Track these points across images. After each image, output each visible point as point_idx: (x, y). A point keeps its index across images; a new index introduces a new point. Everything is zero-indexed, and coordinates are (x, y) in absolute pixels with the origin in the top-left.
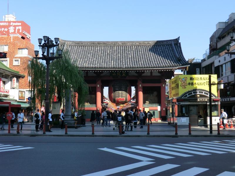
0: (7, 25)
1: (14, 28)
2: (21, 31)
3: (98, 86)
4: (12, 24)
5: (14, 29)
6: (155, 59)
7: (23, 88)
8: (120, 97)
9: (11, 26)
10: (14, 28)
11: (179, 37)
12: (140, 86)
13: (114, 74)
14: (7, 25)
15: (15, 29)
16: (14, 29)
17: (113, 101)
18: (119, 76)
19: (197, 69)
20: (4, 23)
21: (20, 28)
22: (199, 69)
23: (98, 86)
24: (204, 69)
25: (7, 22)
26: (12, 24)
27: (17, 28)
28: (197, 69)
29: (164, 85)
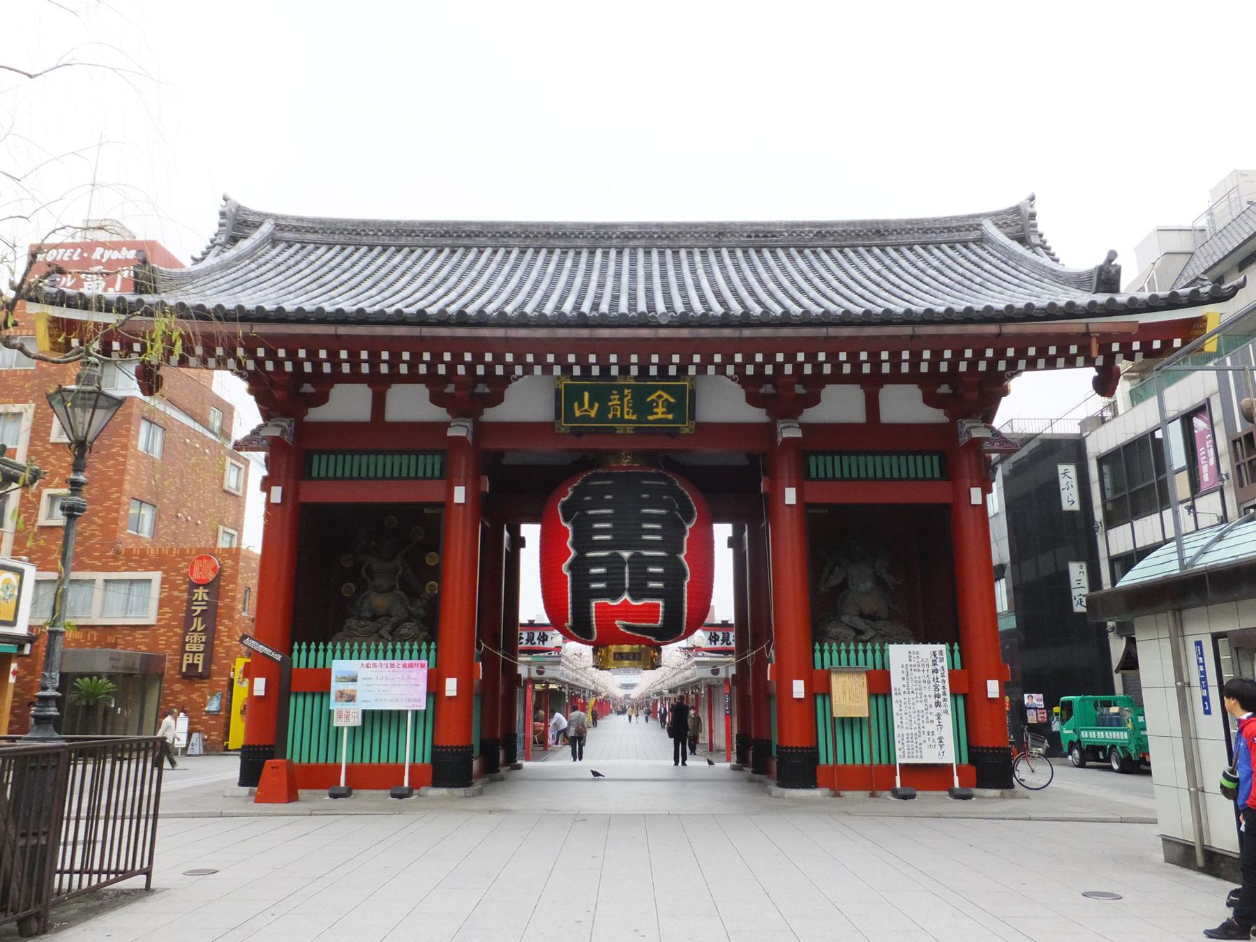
0: (76, 258)
3: (459, 495)
4: (102, 256)
6: (914, 271)
7: (94, 568)
11: (1032, 199)
12: (790, 496)
13: (581, 405)
14: (76, 258)
17: (569, 624)
18: (622, 420)
19: (1061, 468)
20: (62, 251)
22: (1072, 469)
23: (459, 495)
24: (1106, 469)
25: (74, 246)
26: (102, 256)
28: (1061, 468)
29: (976, 495)
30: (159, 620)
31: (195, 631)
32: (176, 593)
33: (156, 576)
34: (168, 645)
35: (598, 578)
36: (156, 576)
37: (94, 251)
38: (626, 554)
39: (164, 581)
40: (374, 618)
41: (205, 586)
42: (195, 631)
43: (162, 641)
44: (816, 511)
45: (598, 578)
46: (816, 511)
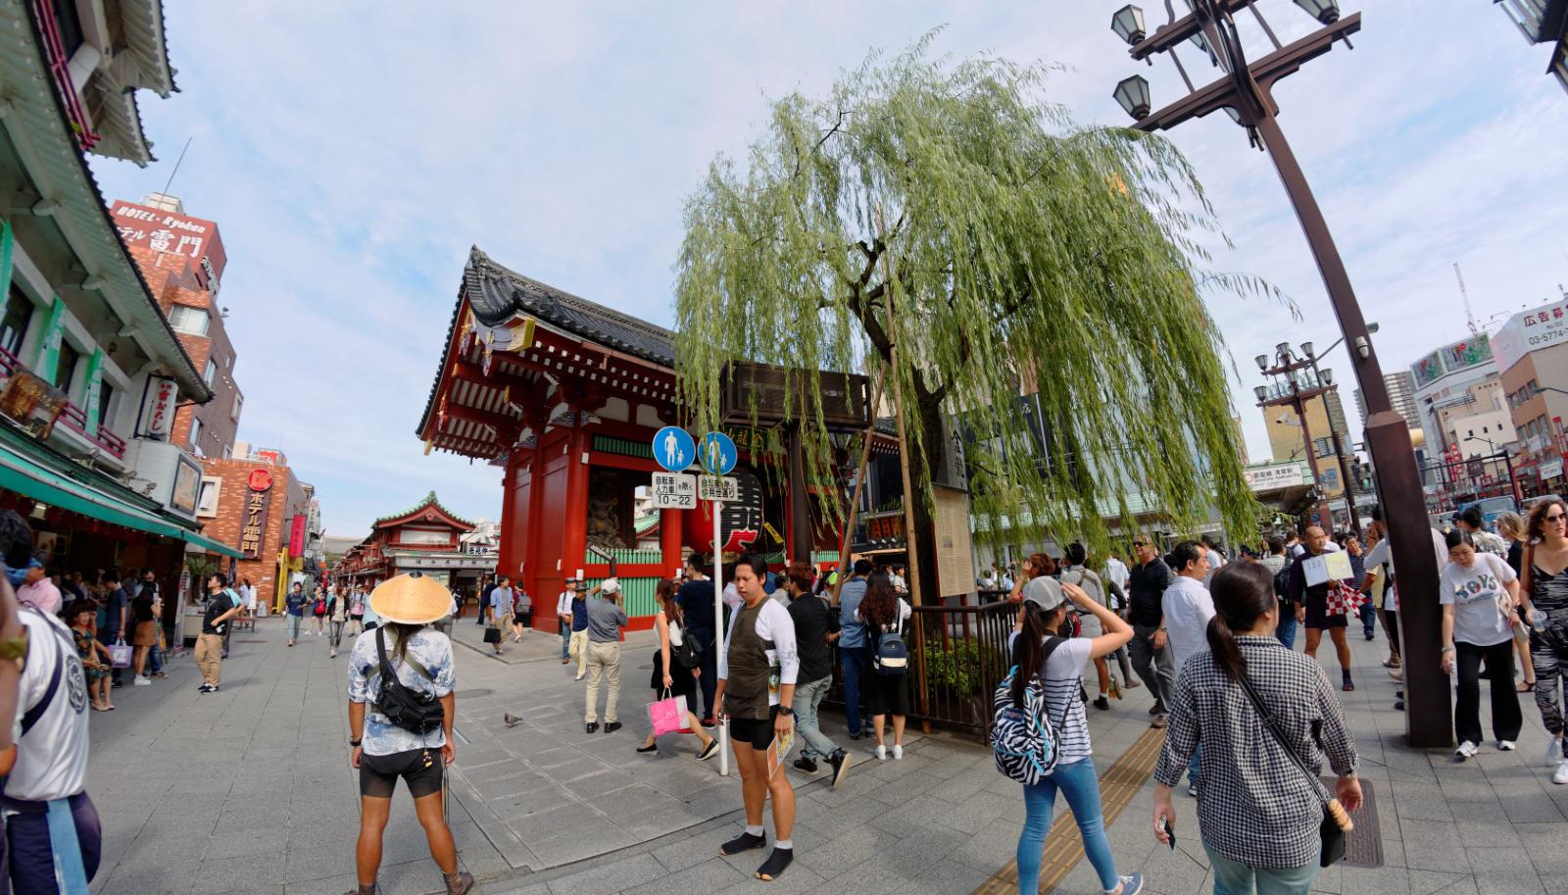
0: (150, 219)
1: (172, 236)
2: (194, 254)
4: (171, 223)
5: (170, 240)
8: (747, 529)
9: (166, 227)
10: (172, 236)
14: (150, 219)
15: (173, 245)
16: (170, 240)
20: (140, 212)
21: (198, 242)
25: (151, 210)
26: (171, 223)
27: (185, 240)
30: (218, 514)
31: (252, 525)
32: (234, 495)
33: (218, 480)
34: (226, 534)
35: (736, 519)
36: (218, 480)
37: (165, 218)
38: (748, 509)
39: (223, 485)
40: (597, 534)
41: (262, 492)
42: (252, 525)
43: (221, 531)
44: (870, 503)
45: (736, 519)
46: (870, 503)
